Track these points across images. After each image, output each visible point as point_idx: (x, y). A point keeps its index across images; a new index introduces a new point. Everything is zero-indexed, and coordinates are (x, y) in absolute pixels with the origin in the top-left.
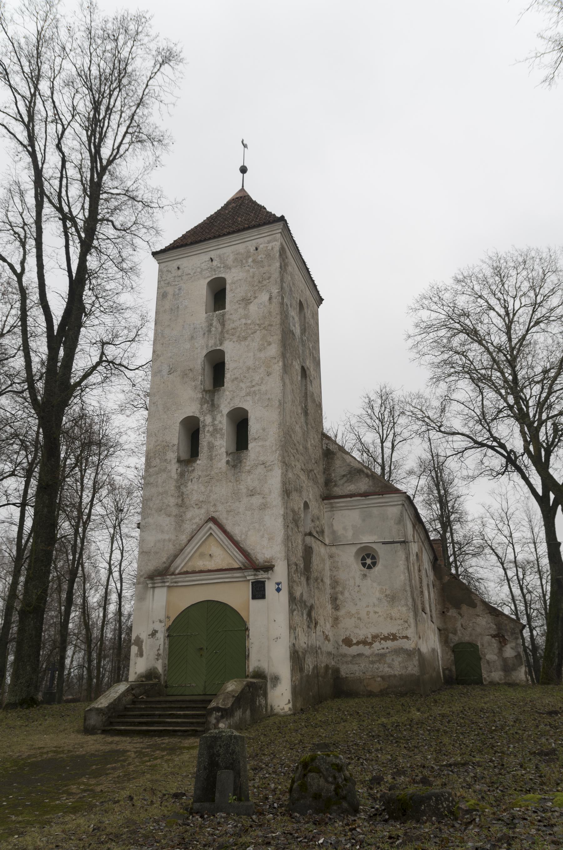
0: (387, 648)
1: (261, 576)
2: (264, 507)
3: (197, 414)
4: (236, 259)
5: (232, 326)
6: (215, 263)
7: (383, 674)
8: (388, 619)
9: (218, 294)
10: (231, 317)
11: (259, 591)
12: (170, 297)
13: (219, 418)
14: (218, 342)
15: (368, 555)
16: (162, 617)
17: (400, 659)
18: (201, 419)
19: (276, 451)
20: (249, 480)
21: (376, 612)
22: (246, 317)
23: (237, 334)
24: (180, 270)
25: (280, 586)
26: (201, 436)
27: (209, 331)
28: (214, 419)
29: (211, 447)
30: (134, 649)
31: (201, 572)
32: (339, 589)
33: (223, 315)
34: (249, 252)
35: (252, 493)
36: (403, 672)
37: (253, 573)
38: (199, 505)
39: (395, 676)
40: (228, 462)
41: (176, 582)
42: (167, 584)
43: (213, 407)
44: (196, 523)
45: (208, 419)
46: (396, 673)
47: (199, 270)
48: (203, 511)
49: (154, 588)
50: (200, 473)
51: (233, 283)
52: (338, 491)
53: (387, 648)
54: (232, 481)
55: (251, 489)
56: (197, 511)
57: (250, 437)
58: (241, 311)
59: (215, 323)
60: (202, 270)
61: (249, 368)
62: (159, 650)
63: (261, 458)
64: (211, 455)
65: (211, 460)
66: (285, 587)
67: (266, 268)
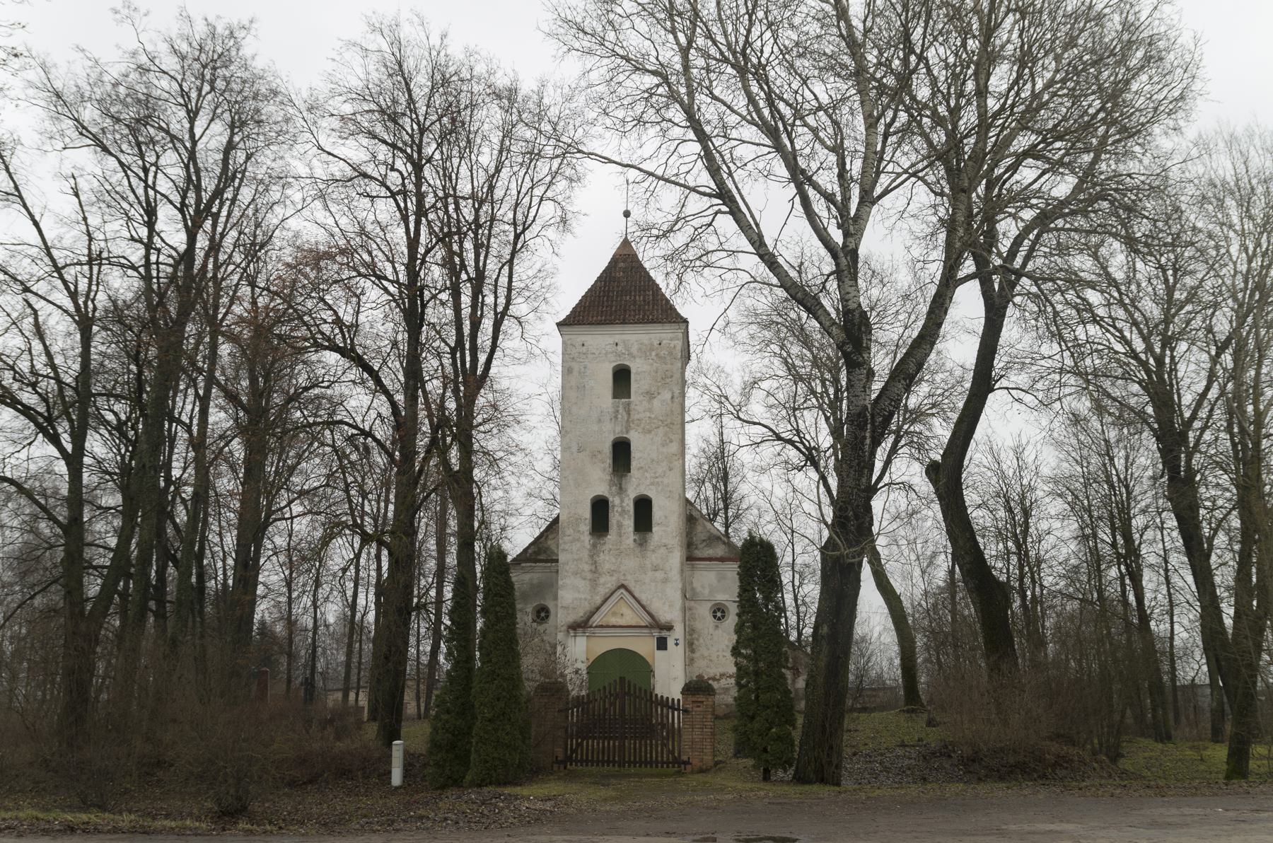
1: (664, 634)
2: (665, 581)
3: (606, 494)
5: (637, 416)
6: (619, 348)
9: (622, 377)
11: (662, 644)
12: (575, 373)
18: (611, 499)
20: (653, 558)
22: (650, 410)
27: (616, 417)
28: (622, 501)
29: (620, 526)
31: (614, 627)
32: (695, 636)
33: (629, 404)
34: (652, 345)
35: (656, 569)
38: (611, 573)
43: (621, 490)
52: (698, 553)
56: (609, 578)
58: (645, 403)
60: (607, 353)
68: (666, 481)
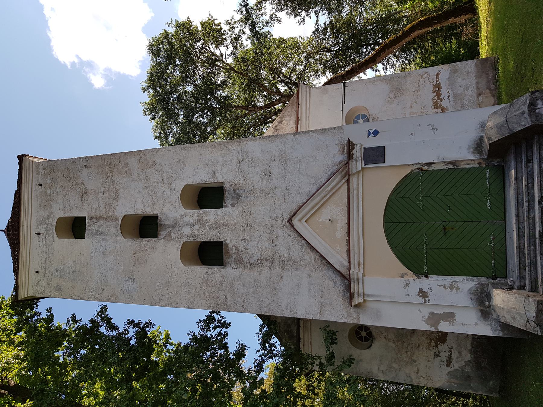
0: (448, 93)
1: (358, 153)
2: (284, 159)
3: (179, 245)
5: (102, 209)
6: (42, 231)
7: (475, 95)
8: (419, 93)
10: (94, 210)
11: (375, 156)
13: (186, 219)
16: (402, 281)
17: (460, 80)
18: (185, 239)
19: (228, 149)
20: (255, 179)
21: (411, 106)
23: (111, 201)
24: (40, 271)
25: (372, 131)
27: (102, 233)
28: (188, 224)
29: (215, 226)
30: (444, 327)
33: (91, 219)
34: (41, 194)
35: (268, 174)
36: (473, 76)
37: (354, 162)
39: (477, 83)
40: (233, 205)
41: (359, 266)
42: (360, 275)
44: (293, 241)
45: (187, 231)
46: (474, 82)
47: (44, 249)
49: (364, 294)
50: (241, 238)
51: (64, 210)
53: (448, 93)
54: (253, 198)
59: (95, 228)
60: (46, 246)
61: (146, 186)
62: (444, 287)
63: (234, 165)
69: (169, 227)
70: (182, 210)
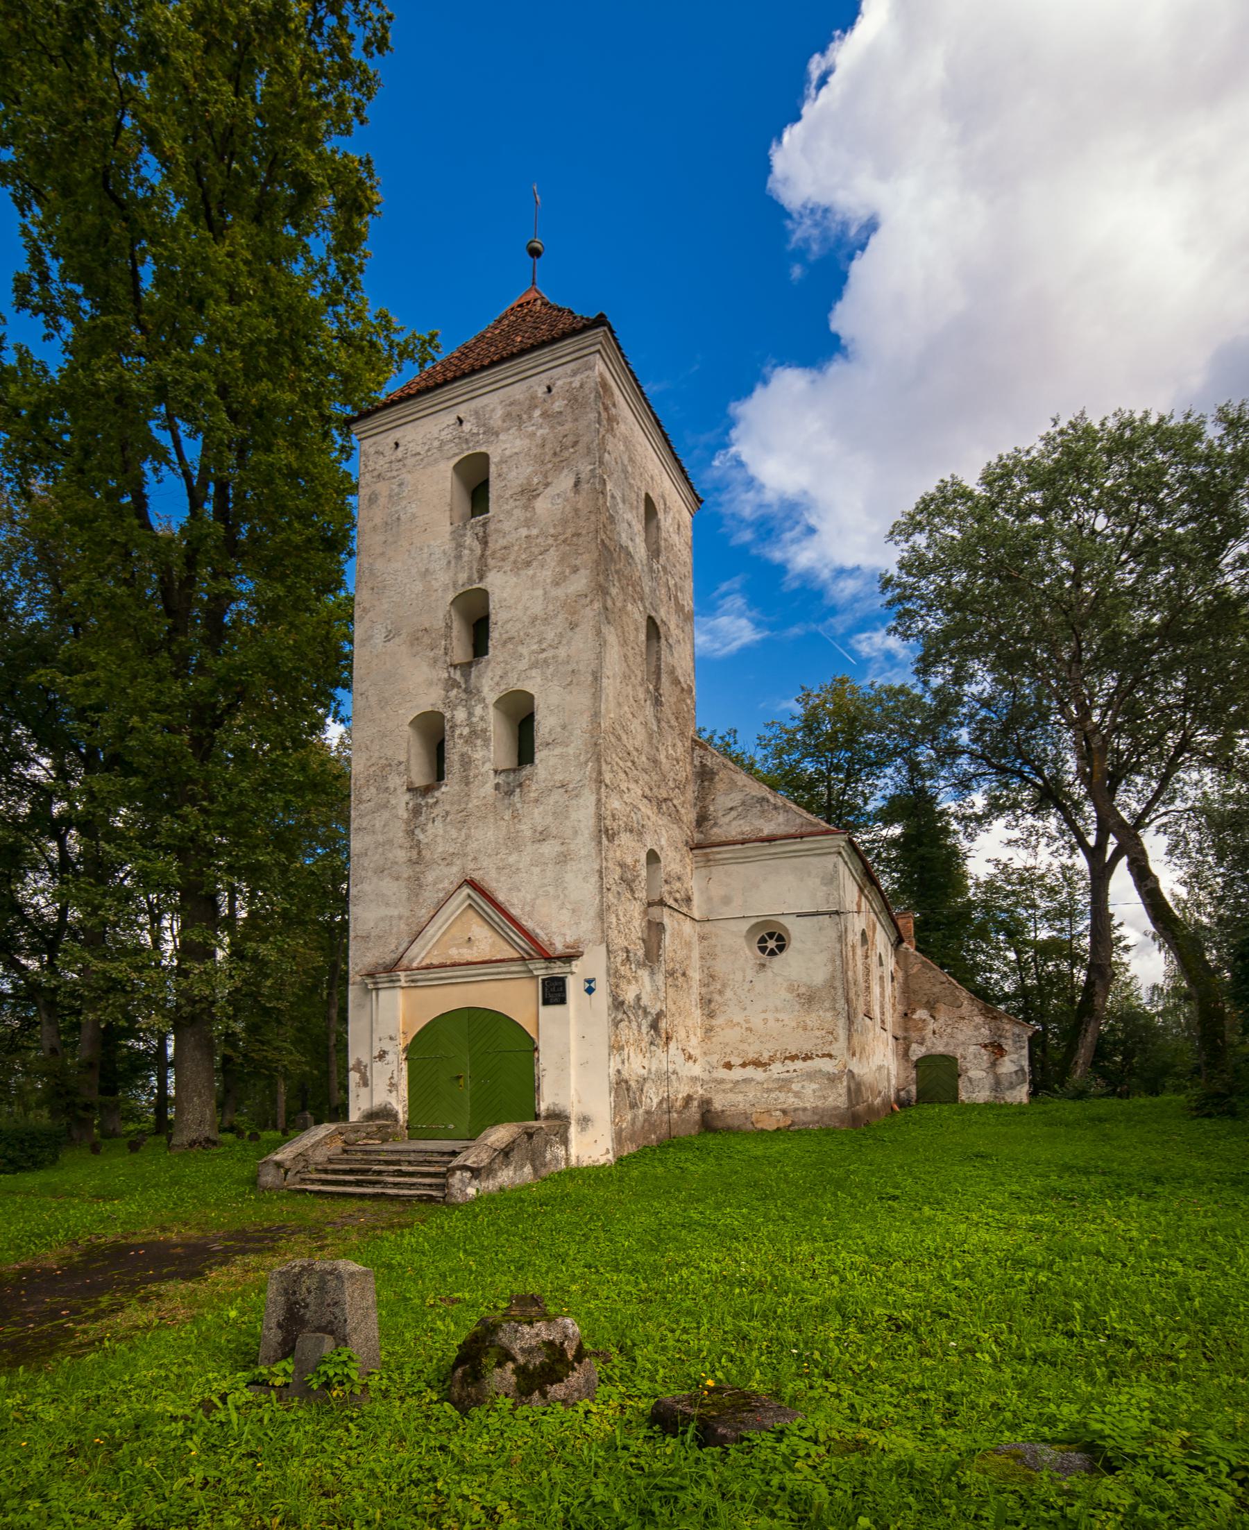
4: (509, 415)
9: (476, 486)
13: (478, 710)
14: (475, 576)
15: (771, 935)
22: (528, 523)
26: (448, 745)
28: (470, 714)
29: (466, 762)
33: (485, 525)
45: (460, 715)
48: (455, 869)
51: (503, 461)
55: (540, 829)
56: (446, 870)
57: (537, 742)
58: (518, 513)
59: (468, 540)
64: (467, 777)
65: (467, 784)
66: (602, 987)
67: (568, 426)
68: (562, 652)
69: (467, 681)
70: (491, 697)
